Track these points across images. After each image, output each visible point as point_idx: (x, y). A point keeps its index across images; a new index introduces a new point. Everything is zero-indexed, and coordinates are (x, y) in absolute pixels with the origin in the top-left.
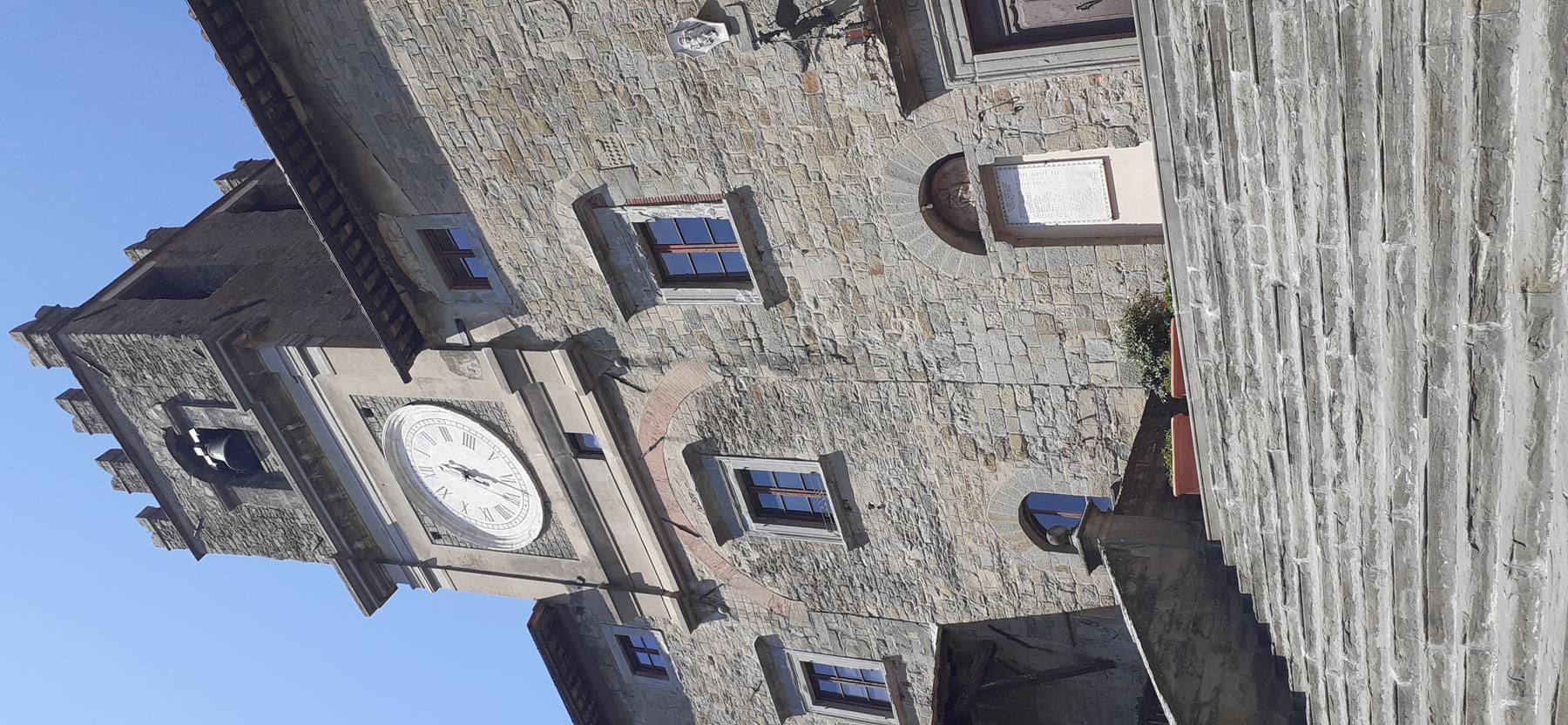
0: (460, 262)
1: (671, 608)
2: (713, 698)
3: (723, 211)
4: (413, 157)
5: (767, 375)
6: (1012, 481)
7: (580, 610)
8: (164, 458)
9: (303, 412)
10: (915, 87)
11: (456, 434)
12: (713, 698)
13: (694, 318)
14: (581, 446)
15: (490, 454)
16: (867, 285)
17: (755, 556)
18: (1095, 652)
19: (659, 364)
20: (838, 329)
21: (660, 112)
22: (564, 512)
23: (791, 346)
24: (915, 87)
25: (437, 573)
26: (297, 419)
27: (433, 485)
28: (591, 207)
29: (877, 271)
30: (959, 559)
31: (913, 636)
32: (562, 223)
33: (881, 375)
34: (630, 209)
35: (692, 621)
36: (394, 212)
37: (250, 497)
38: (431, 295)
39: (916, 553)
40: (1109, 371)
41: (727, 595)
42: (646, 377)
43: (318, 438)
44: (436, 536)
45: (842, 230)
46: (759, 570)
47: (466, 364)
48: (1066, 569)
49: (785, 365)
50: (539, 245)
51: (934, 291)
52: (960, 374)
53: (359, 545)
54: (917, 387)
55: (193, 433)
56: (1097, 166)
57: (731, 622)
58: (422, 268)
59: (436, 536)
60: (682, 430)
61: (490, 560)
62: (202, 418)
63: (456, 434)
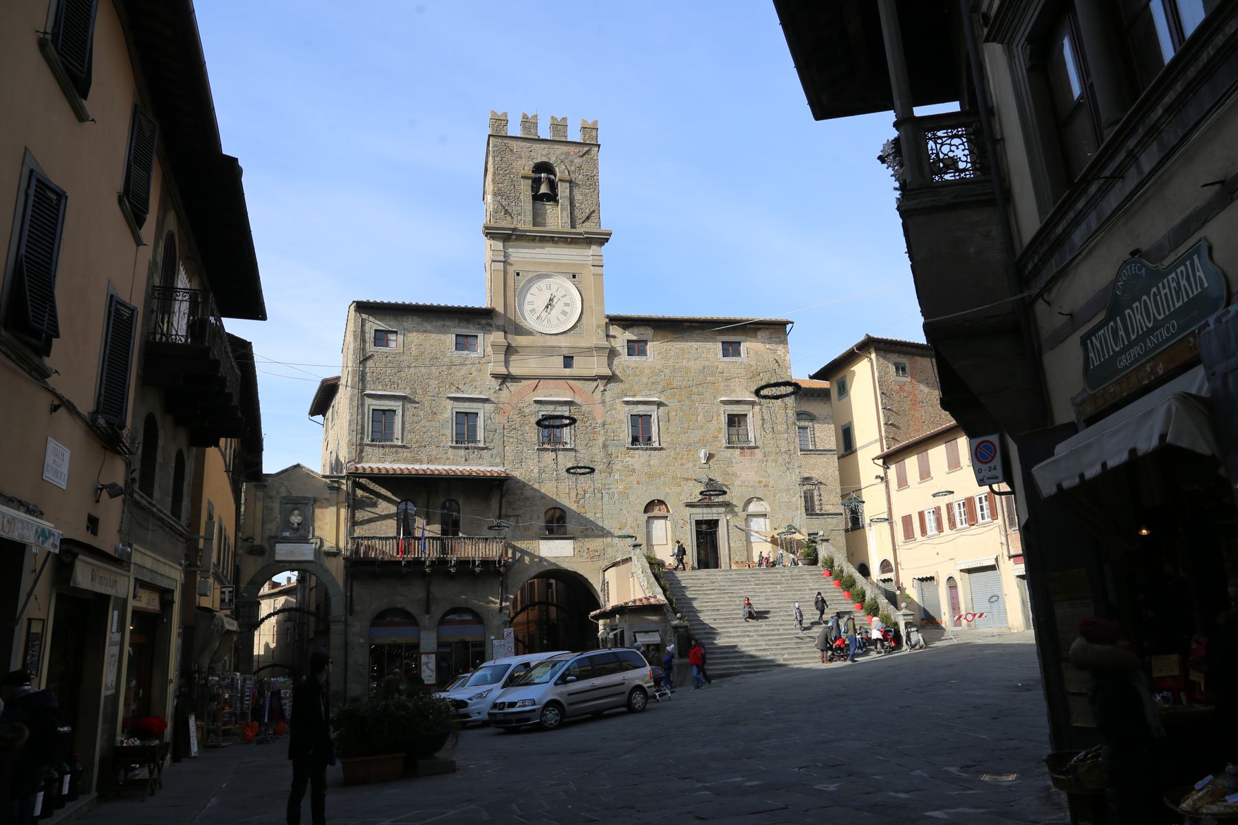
0: (635, 348)
3: (656, 445)
4: (672, 353)
5: (601, 440)
8: (541, 154)
11: (567, 309)
13: (621, 421)
14: (568, 361)
15: (558, 321)
16: (634, 479)
17: (527, 410)
20: (618, 466)
21: (682, 436)
22: (539, 341)
23: (611, 449)
24: (690, 505)
26: (571, 243)
27: (543, 283)
28: (659, 404)
31: (498, 460)
35: (496, 376)
37: (525, 188)
39: (536, 471)
41: (505, 392)
42: (598, 396)
43: (560, 245)
45: (651, 476)
47: (602, 334)
49: (605, 446)
50: (645, 380)
51: (632, 497)
52: (606, 497)
61: (510, 294)
62: (563, 190)
63: (567, 309)
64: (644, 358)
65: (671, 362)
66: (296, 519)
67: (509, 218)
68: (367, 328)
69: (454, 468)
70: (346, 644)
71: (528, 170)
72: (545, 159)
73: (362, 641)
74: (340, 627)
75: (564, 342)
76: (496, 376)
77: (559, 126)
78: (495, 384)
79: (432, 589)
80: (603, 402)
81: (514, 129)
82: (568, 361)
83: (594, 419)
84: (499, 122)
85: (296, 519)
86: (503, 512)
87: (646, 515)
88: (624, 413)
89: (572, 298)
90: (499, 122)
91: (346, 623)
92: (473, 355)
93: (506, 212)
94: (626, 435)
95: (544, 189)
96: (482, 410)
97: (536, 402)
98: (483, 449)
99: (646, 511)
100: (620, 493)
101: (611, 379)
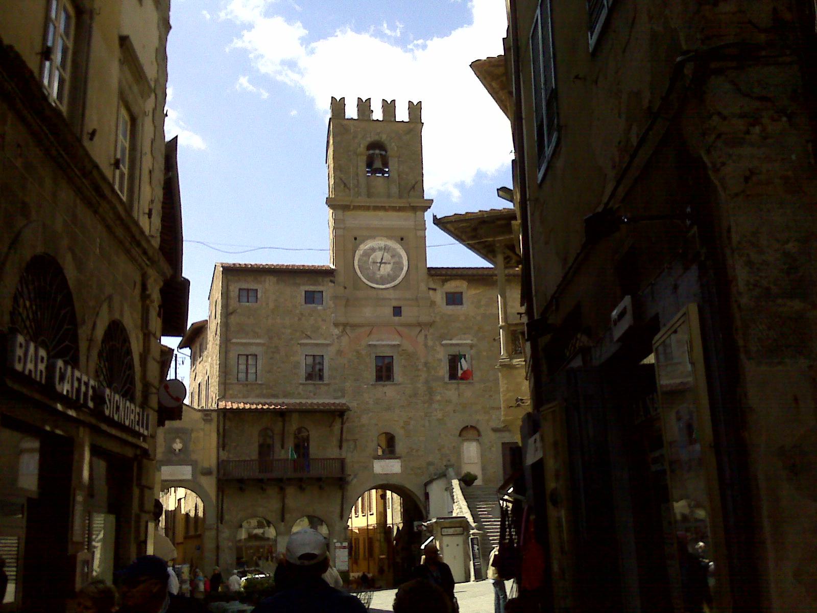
1: (342, 320)
2: (300, 319)
4: (483, 303)
5: (424, 375)
6: (399, 433)
7: (331, 281)
9: (401, 214)
10: (495, 430)
12: (300, 319)
13: (440, 360)
14: (397, 311)
17: (363, 352)
18: (345, 445)
19: (426, 346)
24: (495, 430)
25: (340, 232)
29: (454, 411)
30: (371, 414)
31: (340, 394)
32: (466, 336)
33: (426, 405)
34: (469, 356)
36: (468, 288)
38: (443, 285)
39: (371, 402)
40: (430, 459)
41: (345, 340)
42: (421, 339)
44: (355, 239)
46: (358, 352)
48: (372, 441)
49: (427, 382)
53: (352, 207)
54: (423, 414)
55: (383, 153)
56: (476, 461)
57: (335, 337)
58: (453, 286)
59: (355, 239)
60: (407, 346)
62: (393, 163)
64: (459, 307)
65: (482, 311)
66: (178, 446)
67: (347, 190)
68: (231, 288)
69: (304, 401)
70: (218, 547)
71: (362, 149)
72: (376, 138)
73: (230, 544)
74: (214, 532)
75: (392, 295)
76: (336, 325)
77: (389, 107)
78: (336, 331)
79: (287, 501)
80: (426, 346)
81: (351, 112)
82: (397, 311)
83: (418, 359)
84: (338, 106)
85: (178, 446)
86: (344, 436)
87: (460, 439)
88: (442, 356)
89: (400, 257)
90: (338, 106)
91: (217, 529)
92: (320, 308)
93: (345, 185)
94: (444, 370)
95: (378, 164)
96: (329, 355)
97: (370, 345)
98: (328, 385)
99: (460, 435)
100: (438, 420)
101: (431, 324)
